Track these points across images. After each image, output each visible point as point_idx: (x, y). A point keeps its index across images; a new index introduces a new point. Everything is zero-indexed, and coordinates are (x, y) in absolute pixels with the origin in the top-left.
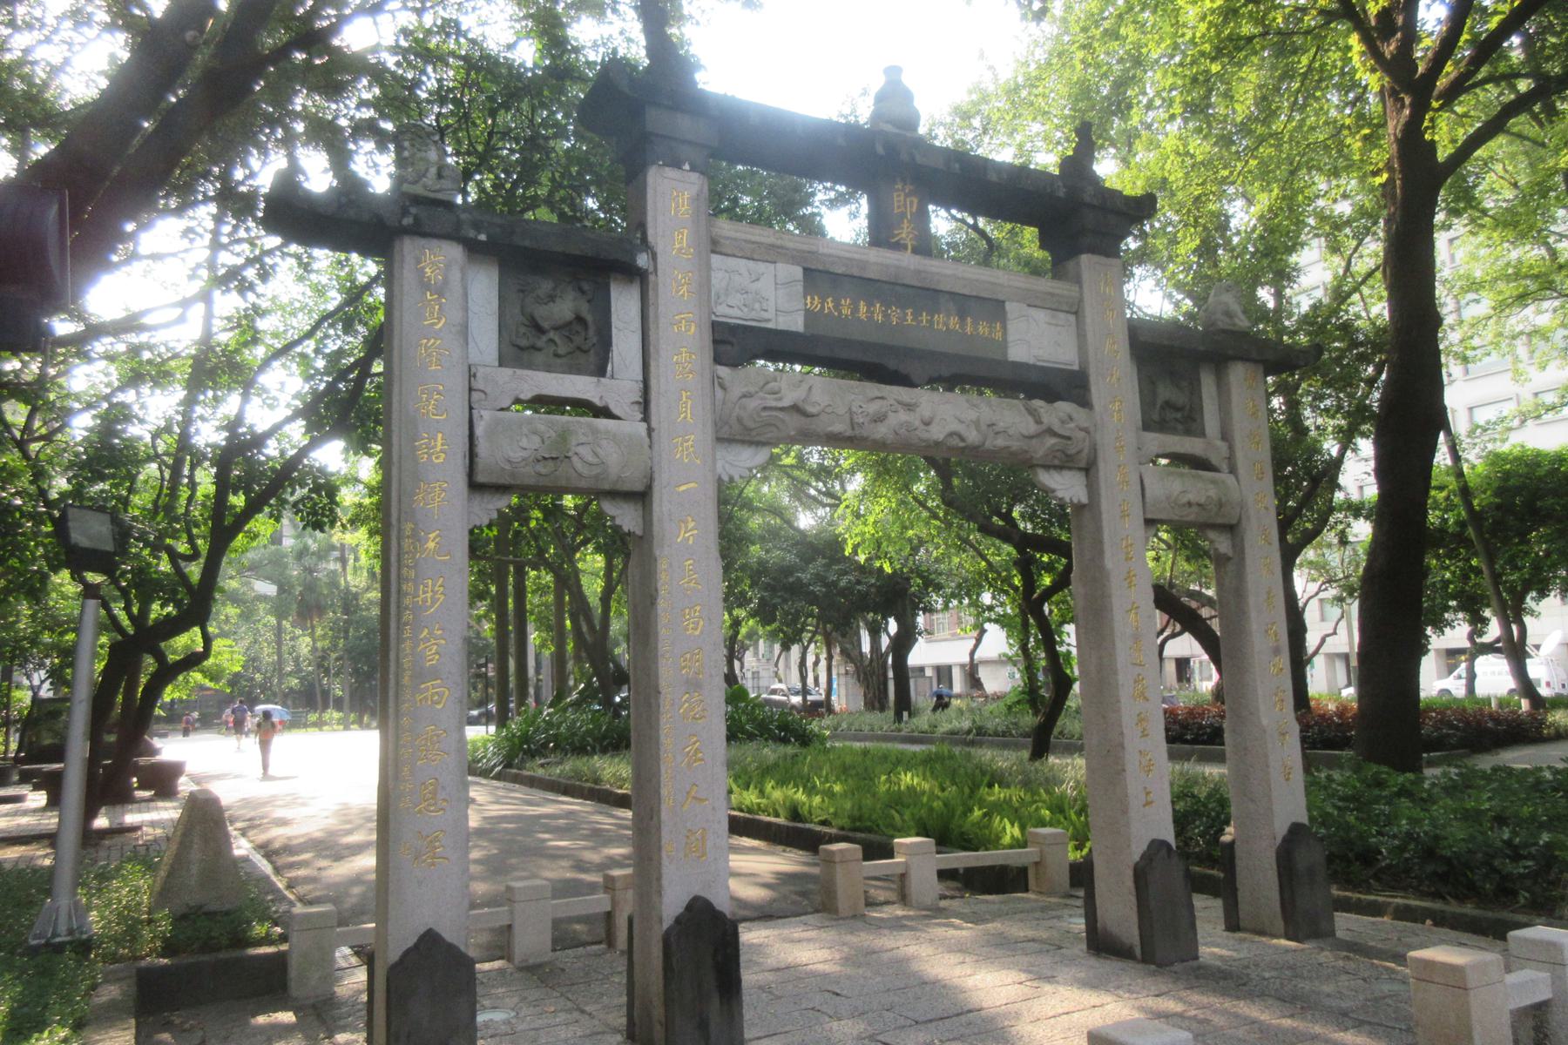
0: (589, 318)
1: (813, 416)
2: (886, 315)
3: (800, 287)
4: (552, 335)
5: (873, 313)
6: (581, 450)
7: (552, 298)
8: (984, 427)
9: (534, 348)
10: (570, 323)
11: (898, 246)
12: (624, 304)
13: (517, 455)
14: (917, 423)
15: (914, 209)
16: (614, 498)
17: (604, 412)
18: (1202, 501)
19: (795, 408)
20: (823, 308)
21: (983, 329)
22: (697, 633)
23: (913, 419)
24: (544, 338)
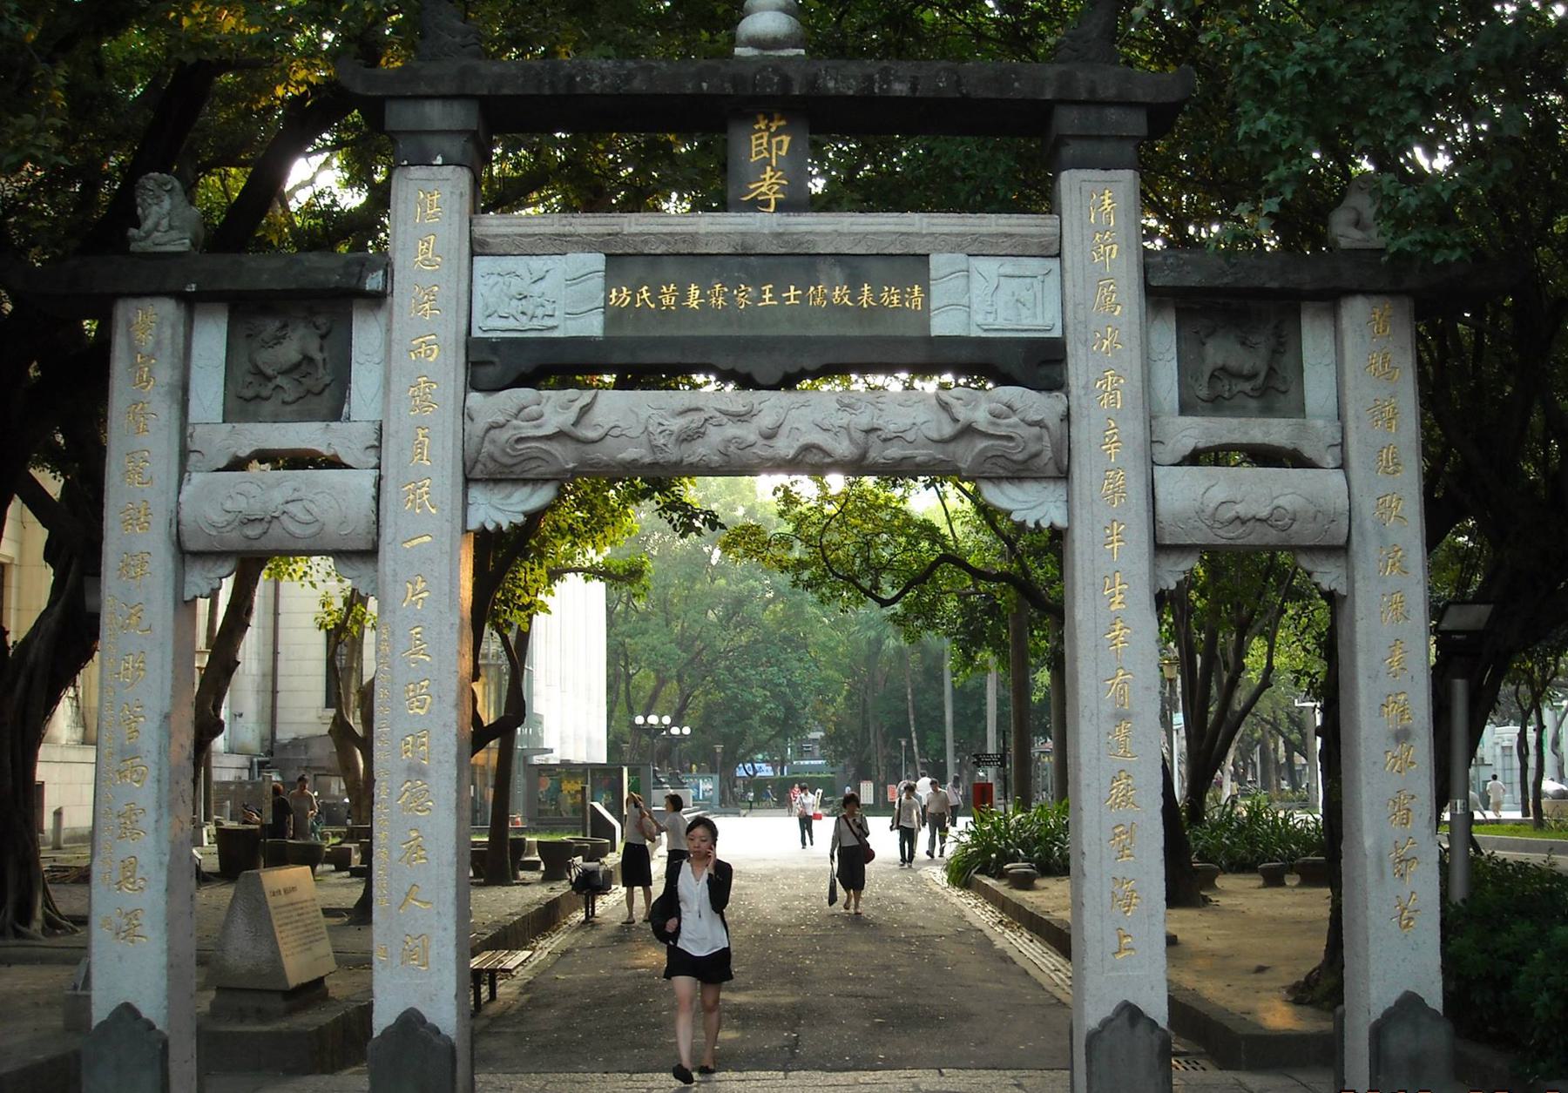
0: (318, 356)
1: (597, 442)
2: (730, 298)
3: (598, 282)
4: (280, 380)
5: (708, 298)
6: (290, 507)
7: (278, 340)
8: (859, 436)
9: (257, 397)
10: (297, 366)
11: (757, 205)
12: (366, 335)
13: (219, 518)
14: (752, 438)
15: (783, 153)
16: (349, 558)
17: (334, 463)
18: (1264, 513)
19: (560, 435)
20: (634, 301)
21: (891, 298)
23: (749, 433)
24: (271, 386)
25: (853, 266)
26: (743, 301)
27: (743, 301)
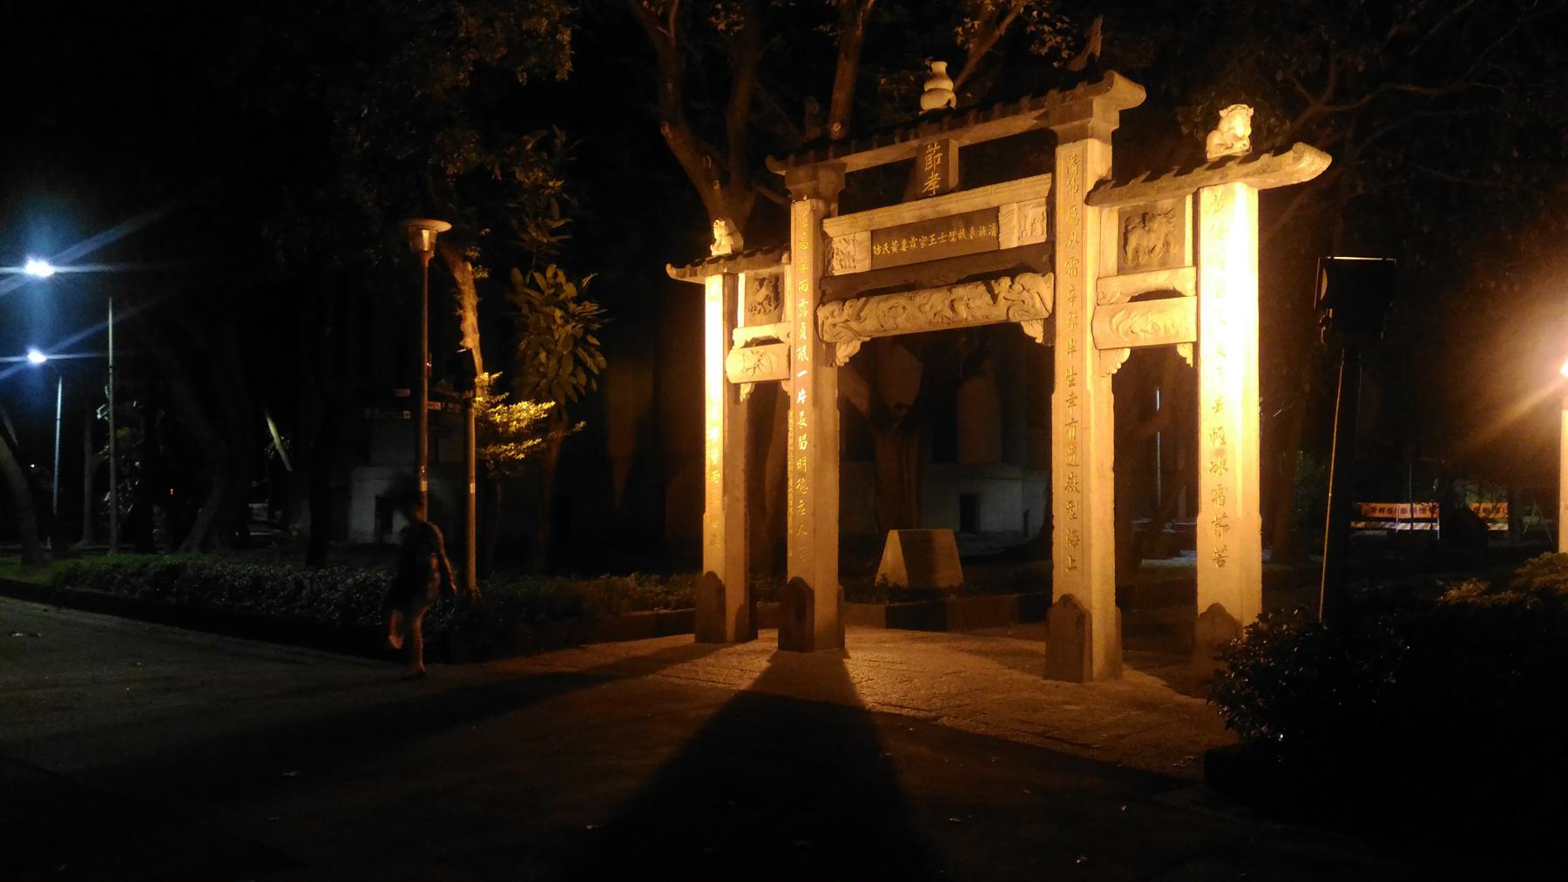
2: (918, 243)
11: (927, 195)
21: (983, 232)
22: (804, 448)
25: (968, 219)
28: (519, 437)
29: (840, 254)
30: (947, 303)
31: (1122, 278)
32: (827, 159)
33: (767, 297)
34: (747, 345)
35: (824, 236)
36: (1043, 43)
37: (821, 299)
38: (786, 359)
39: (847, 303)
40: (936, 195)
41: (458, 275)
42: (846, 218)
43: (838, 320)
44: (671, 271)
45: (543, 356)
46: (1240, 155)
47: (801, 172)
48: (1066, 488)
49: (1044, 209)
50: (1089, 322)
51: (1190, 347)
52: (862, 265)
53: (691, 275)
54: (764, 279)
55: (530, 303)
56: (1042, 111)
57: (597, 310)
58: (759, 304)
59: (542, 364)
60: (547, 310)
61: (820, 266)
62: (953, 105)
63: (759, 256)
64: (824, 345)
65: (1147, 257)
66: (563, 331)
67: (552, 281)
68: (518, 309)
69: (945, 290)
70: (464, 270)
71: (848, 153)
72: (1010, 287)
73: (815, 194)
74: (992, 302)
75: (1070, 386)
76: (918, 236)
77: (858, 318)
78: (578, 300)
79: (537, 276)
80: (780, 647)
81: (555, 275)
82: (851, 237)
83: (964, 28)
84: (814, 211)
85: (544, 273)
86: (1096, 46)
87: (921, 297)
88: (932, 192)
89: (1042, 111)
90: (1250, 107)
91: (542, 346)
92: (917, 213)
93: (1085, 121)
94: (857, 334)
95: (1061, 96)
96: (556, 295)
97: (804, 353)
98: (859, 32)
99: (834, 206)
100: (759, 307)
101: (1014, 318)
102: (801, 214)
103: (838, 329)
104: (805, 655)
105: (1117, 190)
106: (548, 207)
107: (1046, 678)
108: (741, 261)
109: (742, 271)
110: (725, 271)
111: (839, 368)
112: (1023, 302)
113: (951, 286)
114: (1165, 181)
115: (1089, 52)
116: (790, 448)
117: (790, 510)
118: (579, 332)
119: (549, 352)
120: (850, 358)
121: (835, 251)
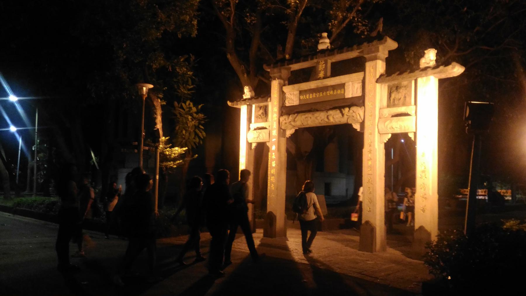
2: (316, 95)
11: (319, 79)
21: (339, 92)
25: (334, 87)
26: (318, 96)
27: (318, 96)
28: (174, 160)
29: (289, 99)
30: (326, 116)
31: (389, 109)
32: (284, 65)
33: (262, 113)
34: (255, 129)
35: (283, 92)
36: (358, 30)
37: (281, 114)
38: (268, 135)
39: (291, 116)
40: (322, 79)
41: (155, 103)
42: (291, 87)
43: (287, 121)
44: (229, 103)
45: (184, 132)
46: (432, 66)
47: (276, 70)
48: (368, 183)
49: (361, 84)
50: (376, 124)
51: (413, 133)
52: (296, 102)
53: (236, 105)
54: (261, 107)
55: (180, 113)
56: (361, 50)
57: (203, 117)
58: (260, 115)
59: (184, 135)
60: (186, 116)
61: (281, 103)
62: (329, 48)
63: (260, 99)
64: (282, 130)
65: (398, 102)
66: (191, 123)
67: (188, 106)
68: (176, 116)
69: (325, 112)
70: (157, 101)
71: (292, 64)
72: (349, 111)
73: (280, 78)
74: (342, 116)
75: (370, 146)
76: (316, 93)
77: (294, 121)
78: (197, 113)
79: (183, 104)
80: (264, 236)
81: (189, 104)
82: (292, 93)
83: (331, 24)
84: (280, 84)
85: (185, 104)
86: (380, 28)
87: (317, 114)
88: (321, 78)
89: (361, 50)
90: (436, 49)
91: (184, 128)
92: (316, 85)
93: (376, 54)
94: (294, 126)
95: (368, 45)
96: (189, 111)
97: (275, 133)
98: (296, 24)
99: (287, 82)
100: (259, 116)
101: (350, 122)
102: (275, 85)
103: (287, 124)
104: (273, 239)
105: (388, 78)
106: (188, 81)
107: (359, 250)
108: (254, 100)
109: (253, 104)
110: (248, 104)
111: (287, 138)
112: (353, 116)
113: (327, 110)
114: (405, 75)
115: (378, 30)
116: (269, 166)
117: (269, 188)
118: (197, 124)
119: (186, 130)
120: (291, 135)
121: (287, 97)
